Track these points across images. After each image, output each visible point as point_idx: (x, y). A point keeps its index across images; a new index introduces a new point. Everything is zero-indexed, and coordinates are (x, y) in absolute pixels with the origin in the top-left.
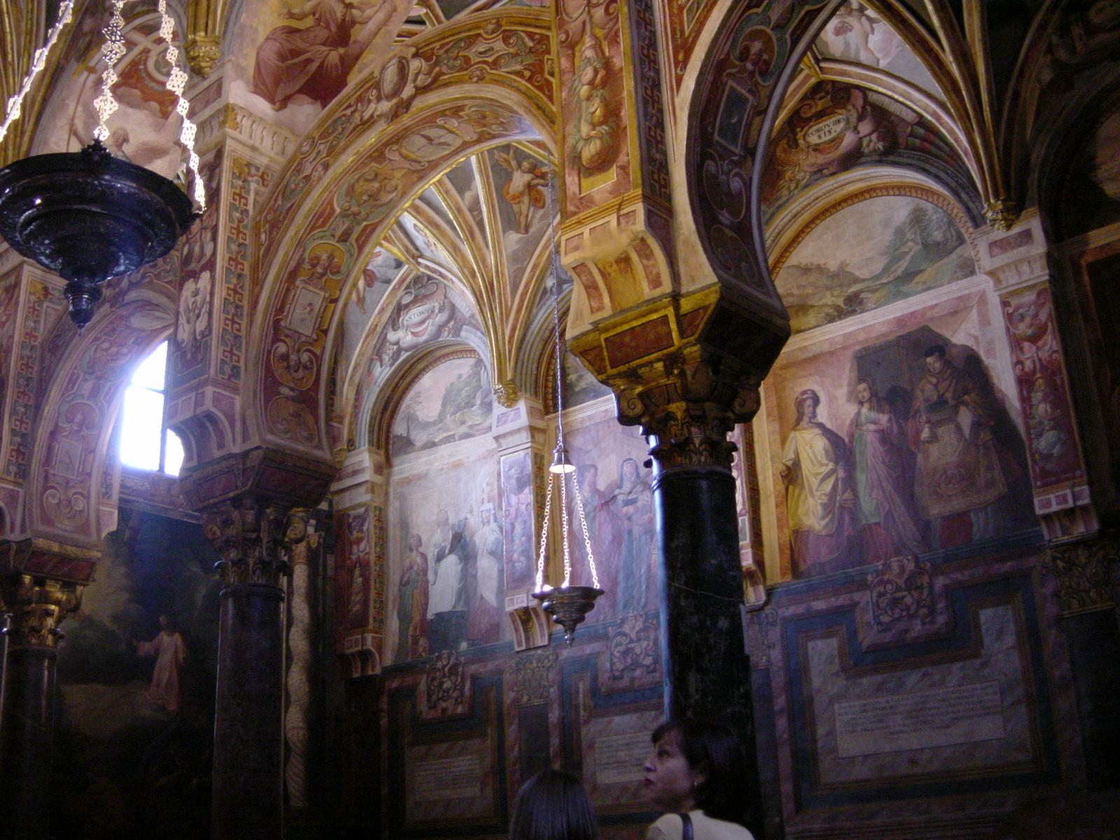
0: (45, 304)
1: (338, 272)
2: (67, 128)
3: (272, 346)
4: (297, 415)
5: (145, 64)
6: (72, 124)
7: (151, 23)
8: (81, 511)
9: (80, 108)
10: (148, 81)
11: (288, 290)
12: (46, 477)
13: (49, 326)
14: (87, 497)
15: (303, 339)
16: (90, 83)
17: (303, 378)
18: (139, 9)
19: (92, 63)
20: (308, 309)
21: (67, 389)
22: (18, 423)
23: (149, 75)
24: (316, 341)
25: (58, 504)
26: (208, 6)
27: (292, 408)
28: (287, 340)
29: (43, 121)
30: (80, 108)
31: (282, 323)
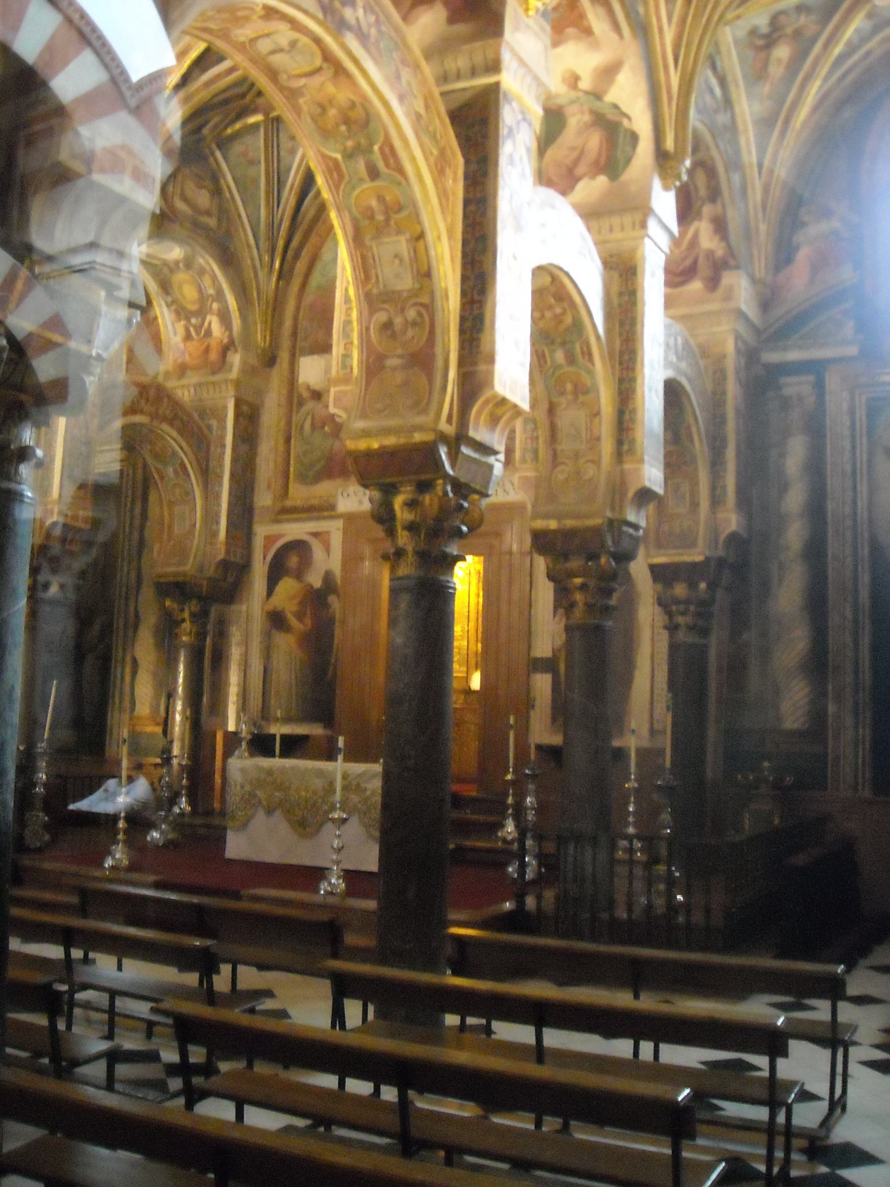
1: (400, 209)
3: (370, 322)
4: (406, 383)
8: (590, 480)
11: (364, 258)
12: (555, 455)
14: (597, 463)
15: (405, 294)
17: (413, 337)
20: (397, 262)
24: (421, 289)
25: (567, 479)
27: (399, 378)
28: (386, 306)
31: (375, 291)
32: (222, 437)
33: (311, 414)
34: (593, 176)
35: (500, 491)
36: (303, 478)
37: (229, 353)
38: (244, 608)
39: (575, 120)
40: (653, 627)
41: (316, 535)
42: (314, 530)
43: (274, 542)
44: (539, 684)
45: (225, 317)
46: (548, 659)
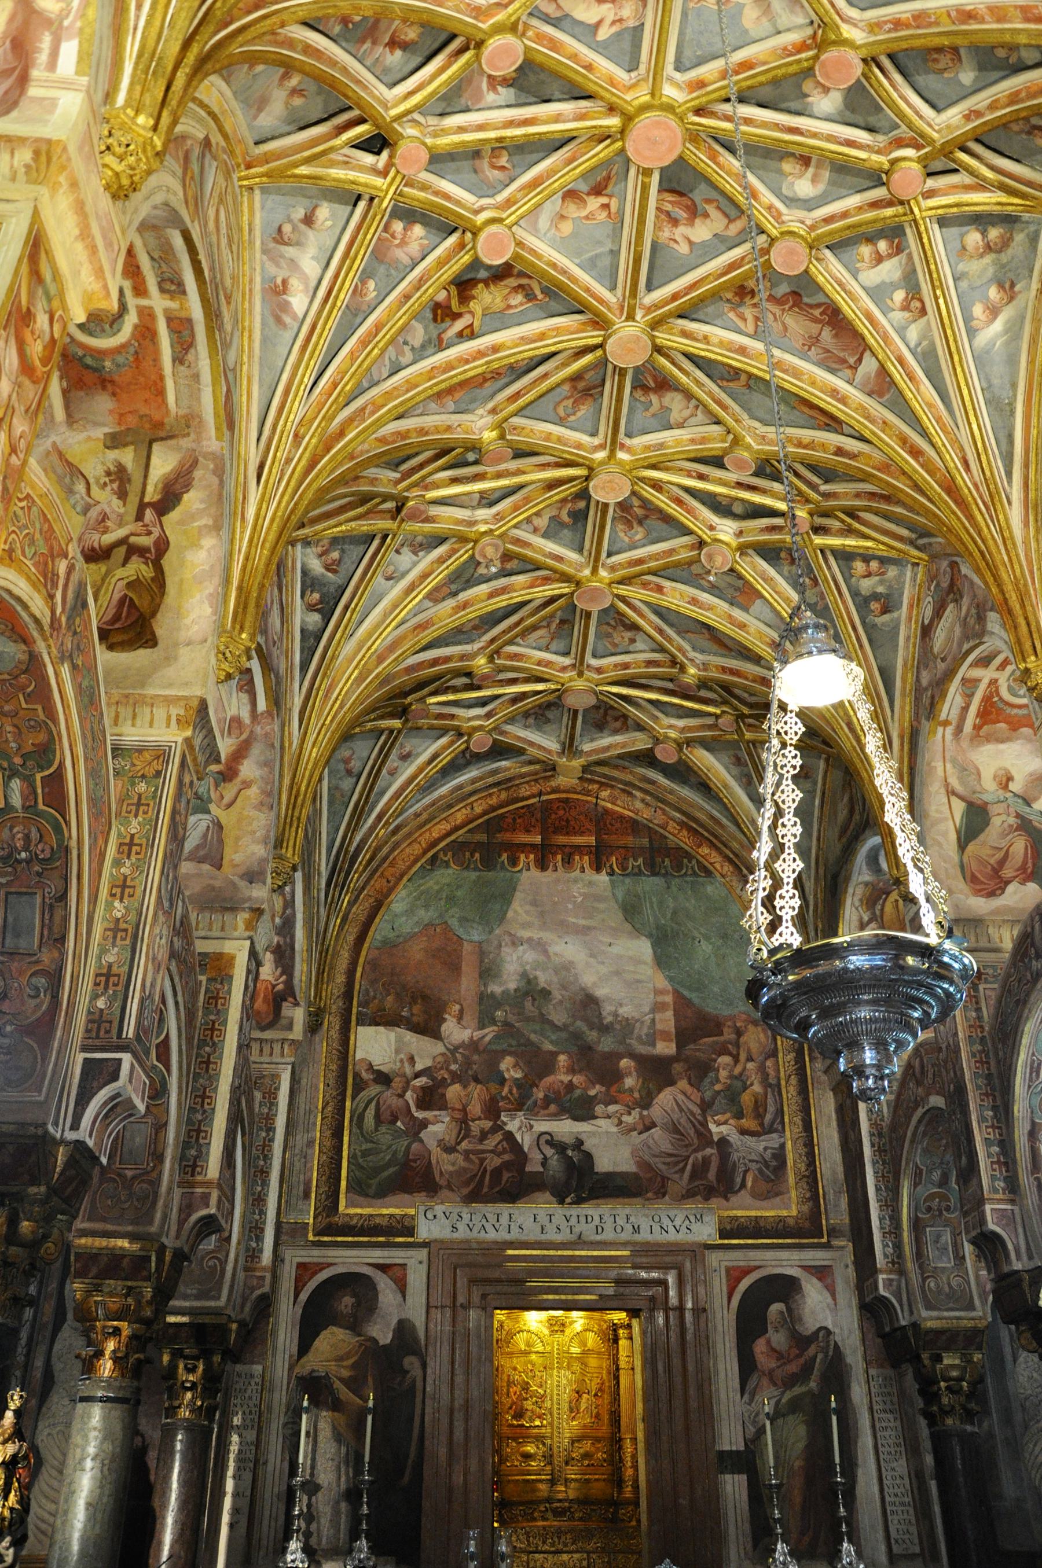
0: (981, 987)
2: (943, 791)
5: (998, 694)
6: (947, 785)
7: (985, 654)
9: (948, 766)
10: (1009, 710)
13: (992, 1010)
16: (949, 736)
18: (966, 647)
19: (943, 716)
21: (1031, 1079)
22: (990, 1130)
23: (1007, 704)
26: (1028, 625)
29: (916, 794)
30: (948, 766)
32: (269, 1119)
33: (374, 1103)
34: (1023, 883)
35: (656, 1228)
36: (358, 1188)
37: (285, 1004)
38: (258, 1369)
39: (1000, 821)
40: (871, 1409)
41: (383, 1268)
42: (381, 1261)
43: (315, 1273)
44: (729, 1488)
45: (284, 955)
46: (738, 1452)
